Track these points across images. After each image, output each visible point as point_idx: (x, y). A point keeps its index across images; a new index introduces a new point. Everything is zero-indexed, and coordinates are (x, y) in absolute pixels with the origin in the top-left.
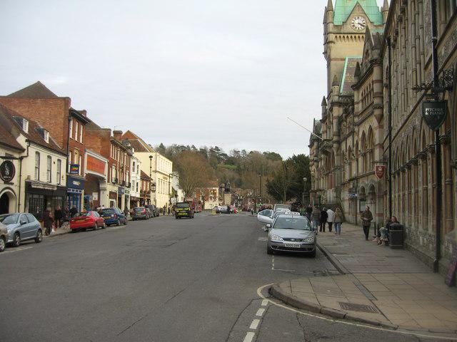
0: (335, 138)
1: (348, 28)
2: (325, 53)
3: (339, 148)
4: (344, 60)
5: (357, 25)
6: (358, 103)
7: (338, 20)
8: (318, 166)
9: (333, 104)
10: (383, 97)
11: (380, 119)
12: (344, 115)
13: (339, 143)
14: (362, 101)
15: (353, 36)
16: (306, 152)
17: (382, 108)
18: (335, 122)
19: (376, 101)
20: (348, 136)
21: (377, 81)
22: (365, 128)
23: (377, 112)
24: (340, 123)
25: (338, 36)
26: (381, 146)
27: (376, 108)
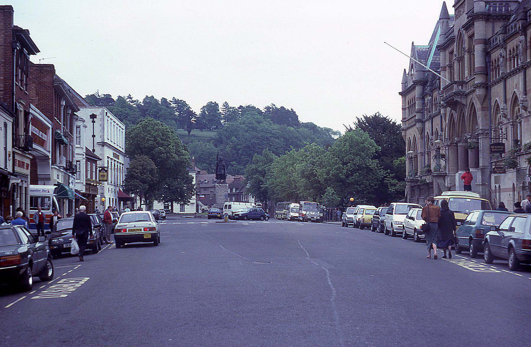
0: (478, 80)
3: (487, 97)
8: (422, 130)
9: (473, 17)
12: (500, 37)
13: (487, 87)
18: (478, 49)
20: (513, 73)
24: (487, 54)
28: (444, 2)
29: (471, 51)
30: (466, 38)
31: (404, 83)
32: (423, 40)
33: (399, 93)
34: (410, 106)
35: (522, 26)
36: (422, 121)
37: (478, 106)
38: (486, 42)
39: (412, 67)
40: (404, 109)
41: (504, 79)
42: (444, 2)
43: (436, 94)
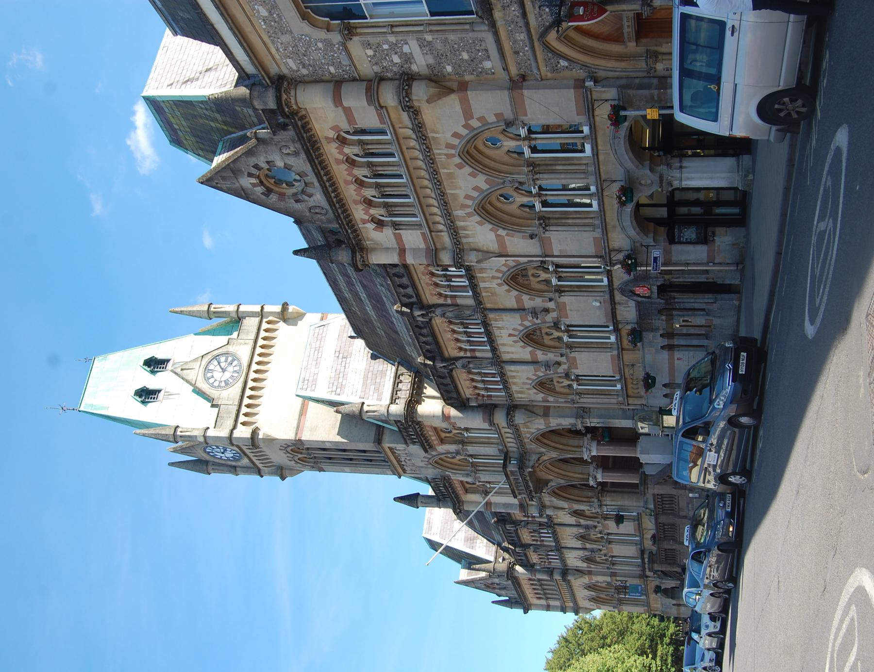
0: (500, 418)
2: (282, 472)
3: (529, 409)
6: (402, 251)
8: (579, 571)
14: (396, 226)
19: (389, 96)
21: (337, 100)
22: (465, 184)
23: (420, 92)
25: (242, 419)
26: (518, 84)
28: (395, 499)
30: (442, 448)
31: (510, 603)
33: (525, 612)
34: (545, 594)
35: (421, 308)
36: (565, 572)
37: (539, 425)
40: (548, 608)
41: (497, 361)
42: (395, 499)
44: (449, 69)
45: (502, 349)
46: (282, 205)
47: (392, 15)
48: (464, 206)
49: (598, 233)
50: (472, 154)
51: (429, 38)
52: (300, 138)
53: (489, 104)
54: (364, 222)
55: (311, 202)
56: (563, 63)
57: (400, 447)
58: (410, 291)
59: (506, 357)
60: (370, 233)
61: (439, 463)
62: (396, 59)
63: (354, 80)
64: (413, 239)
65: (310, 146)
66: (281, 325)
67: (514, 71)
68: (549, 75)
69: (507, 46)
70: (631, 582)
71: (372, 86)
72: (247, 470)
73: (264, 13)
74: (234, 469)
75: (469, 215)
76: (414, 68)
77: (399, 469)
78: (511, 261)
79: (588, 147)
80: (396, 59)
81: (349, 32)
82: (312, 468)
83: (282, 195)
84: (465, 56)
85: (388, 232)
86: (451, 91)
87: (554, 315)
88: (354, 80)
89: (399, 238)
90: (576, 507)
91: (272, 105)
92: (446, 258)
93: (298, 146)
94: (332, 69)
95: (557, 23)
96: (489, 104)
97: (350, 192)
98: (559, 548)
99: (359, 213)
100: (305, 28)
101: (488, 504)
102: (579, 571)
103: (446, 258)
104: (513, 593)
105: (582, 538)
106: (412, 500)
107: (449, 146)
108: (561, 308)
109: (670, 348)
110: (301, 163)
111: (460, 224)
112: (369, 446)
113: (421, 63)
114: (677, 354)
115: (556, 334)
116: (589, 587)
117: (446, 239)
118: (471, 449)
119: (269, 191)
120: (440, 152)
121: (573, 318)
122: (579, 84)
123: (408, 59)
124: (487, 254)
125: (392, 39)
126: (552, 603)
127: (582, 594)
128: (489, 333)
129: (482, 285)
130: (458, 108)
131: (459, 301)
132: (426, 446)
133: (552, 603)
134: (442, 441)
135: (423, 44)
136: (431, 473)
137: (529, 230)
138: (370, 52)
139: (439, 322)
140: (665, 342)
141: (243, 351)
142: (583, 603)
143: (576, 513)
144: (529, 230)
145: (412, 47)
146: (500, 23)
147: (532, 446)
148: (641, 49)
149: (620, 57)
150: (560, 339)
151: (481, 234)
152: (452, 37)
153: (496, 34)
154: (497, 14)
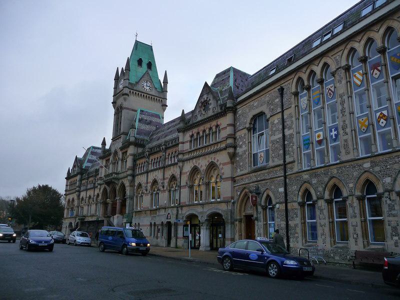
0: (130, 172)
1: (139, 87)
3: (133, 181)
4: (136, 111)
5: (145, 87)
6: (183, 143)
7: (133, 80)
8: (79, 196)
10: (235, 139)
11: (233, 156)
13: (133, 176)
14: (191, 141)
15: (143, 94)
16: (60, 185)
17: (235, 147)
19: (230, 141)
21: (229, 125)
23: (231, 150)
24: (135, 161)
25: (132, 91)
26: (233, 180)
27: (230, 147)
29: (123, 160)
30: (120, 154)
32: (81, 156)
36: (79, 191)
38: (134, 155)
39: (74, 166)
43: (90, 179)
44: (238, 159)
45: (152, 173)
46: (198, 107)
47: (254, 142)
48: (196, 162)
49: (187, 203)
50: (212, 166)
51: (247, 153)
52: (218, 114)
53: (227, 171)
54: (192, 132)
55: (199, 116)
56: (239, 193)
57: (121, 140)
58: (171, 145)
59: (149, 174)
60: (189, 133)
61: (116, 153)
62: (241, 143)
63: (235, 130)
64: (186, 147)
65: (217, 116)
66: (161, 104)
67: (236, 178)
68: (235, 189)
69: (244, 176)
70: (75, 212)
71: (233, 136)
72: (115, 92)
73: (255, 104)
74: (115, 88)
75: (194, 164)
76: (238, 148)
77: (114, 139)
78: (179, 176)
79: (213, 200)
80: (241, 143)
81: (249, 130)
82: (115, 112)
83: (201, 107)
84: (241, 164)
85: (189, 139)
86: (231, 159)
87: (162, 189)
88: (235, 130)
89: (187, 142)
90: (100, 195)
91: (228, 106)
92: (180, 157)
93: (216, 113)
94: (238, 124)
95: (251, 192)
96: (227, 171)
97: (201, 128)
98: (87, 190)
99: (195, 130)
100: (251, 116)
101: (102, 167)
102: (79, 196)
103: (180, 157)
104: (72, 175)
105: (90, 197)
106: (104, 143)
107: (214, 159)
108: (164, 191)
109: (151, 224)
110: (210, 113)
111: (191, 161)
112: (122, 131)
113: (239, 150)
114: (149, 227)
115: (156, 190)
116: (73, 200)
117: (187, 157)
118: (120, 162)
119: (202, 103)
120: (213, 156)
121: (161, 195)
122: (232, 198)
123: (241, 147)
124: (181, 169)
125: (247, 142)
126: (69, 187)
127: (71, 197)
128: (156, 169)
129: (172, 167)
130: (226, 161)
131: (167, 160)
132: (121, 149)
133: (69, 187)
134: (123, 153)
135: (245, 151)
136: (113, 150)
137: (188, 182)
138: (243, 135)
139: (161, 154)
140: (153, 224)
141: (153, 93)
142: (68, 197)
143: (98, 195)
144: (188, 182)
145: (244, 148)
146: (251, 175)
147: (120, 181)
148: (243, 217)
149: (240, 210)
150: (173, 187)
151: (188, 167)
152: (247, 160)
153: (248, 174)
154: (253, 174)
